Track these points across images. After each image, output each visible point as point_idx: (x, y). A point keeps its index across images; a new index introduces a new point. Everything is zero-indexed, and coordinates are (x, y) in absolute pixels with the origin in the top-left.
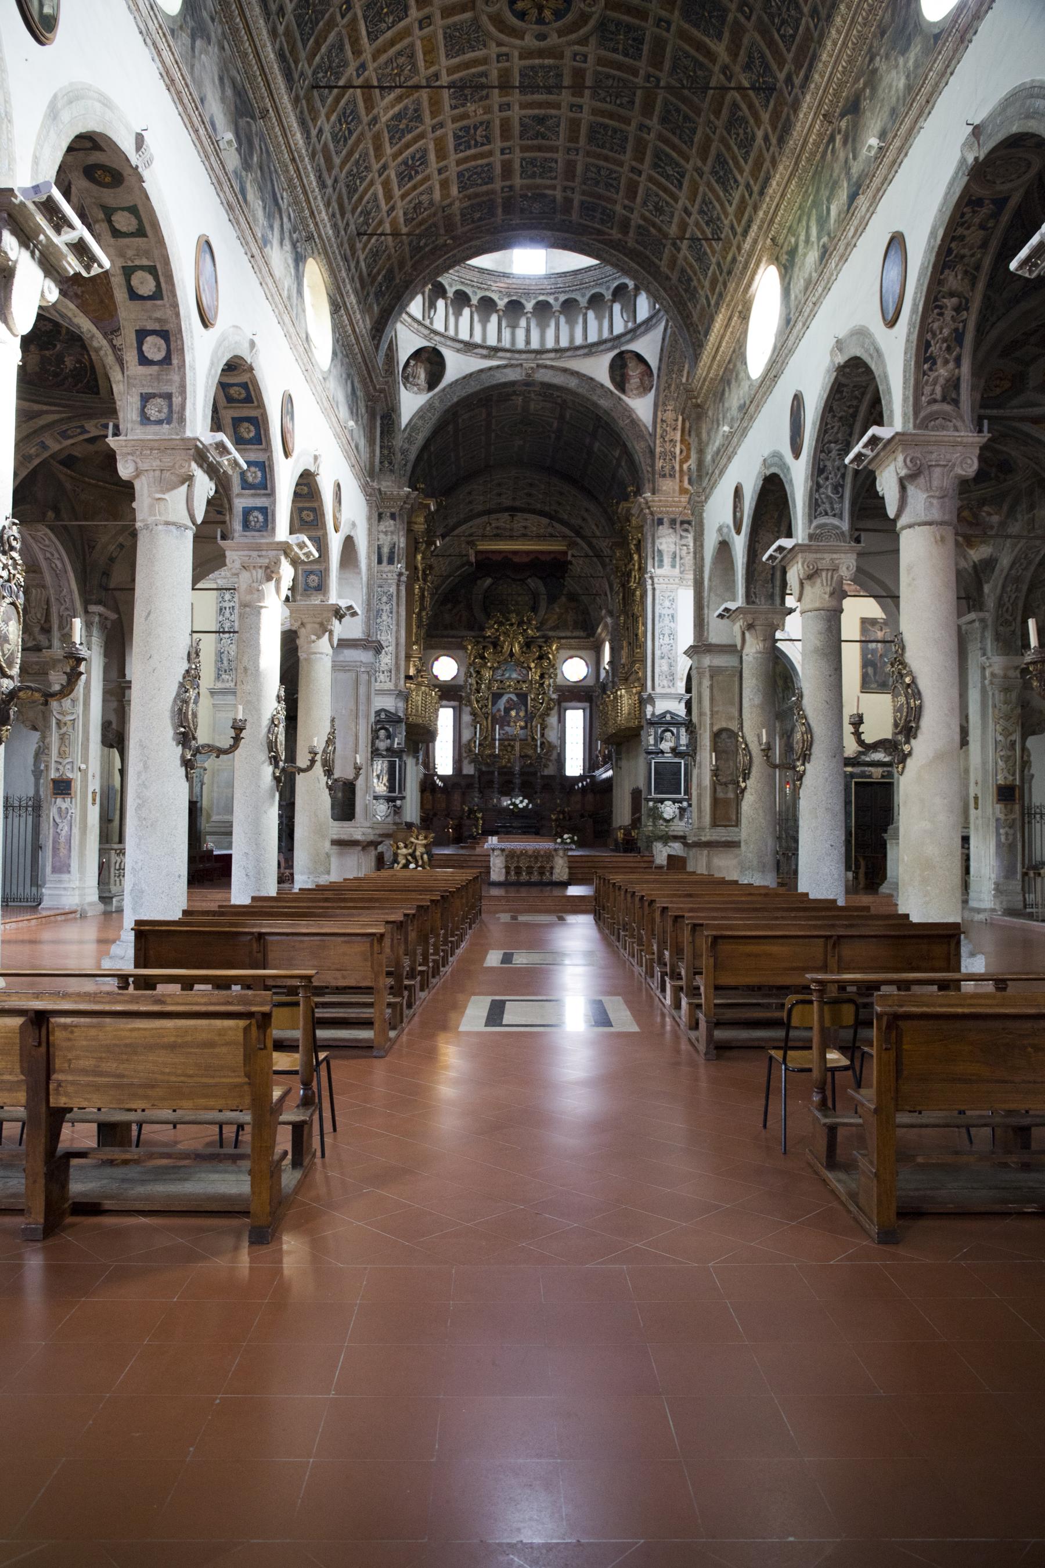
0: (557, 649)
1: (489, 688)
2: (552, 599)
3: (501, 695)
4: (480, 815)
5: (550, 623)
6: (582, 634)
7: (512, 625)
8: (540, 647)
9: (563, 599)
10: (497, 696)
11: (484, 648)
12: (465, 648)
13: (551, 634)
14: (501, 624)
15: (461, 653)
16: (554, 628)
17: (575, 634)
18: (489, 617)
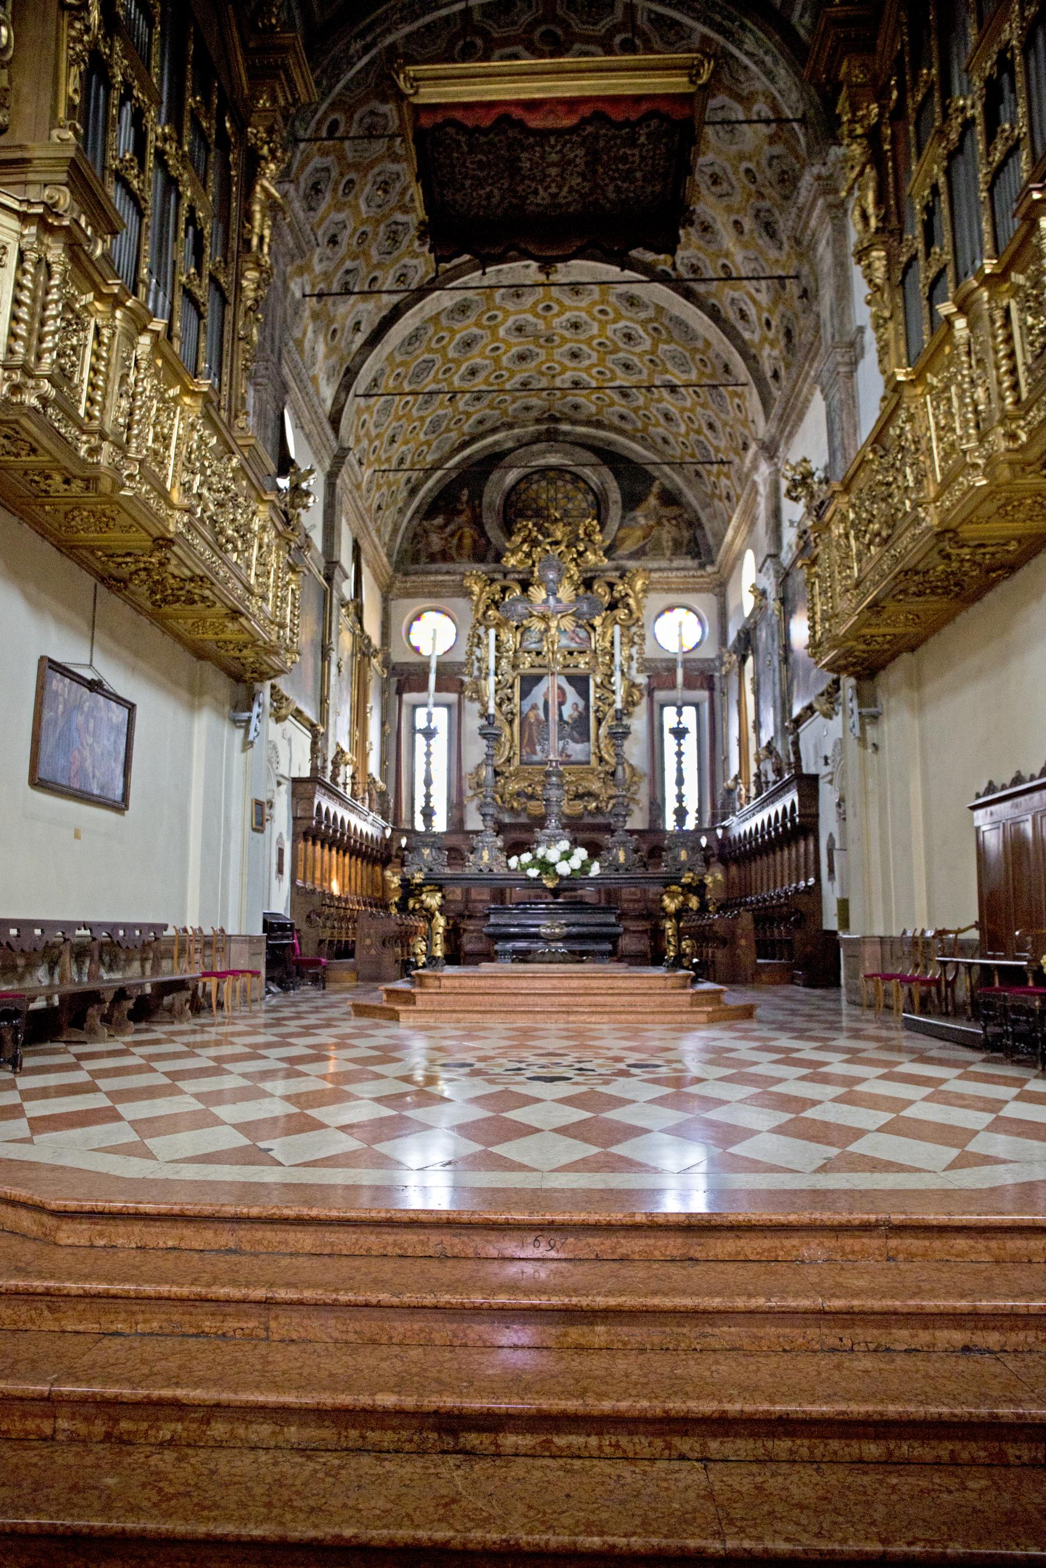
0: (645, 591)
1: (515, 667)
2: (631, 502)
3: (538, 679)
4: (433, 900)
5: (630, 546)
6: (690, 563)
7: (557, 543)
8: (611, 586)
9: (652, 501)
10: (530, 682)
11: (504, 590)
12: (468, 593)
13: (630, 564)
14: (535, 543)
15: (461, 603)
16: (638, 554)
17: (676, 564)
18: (509, 533)
